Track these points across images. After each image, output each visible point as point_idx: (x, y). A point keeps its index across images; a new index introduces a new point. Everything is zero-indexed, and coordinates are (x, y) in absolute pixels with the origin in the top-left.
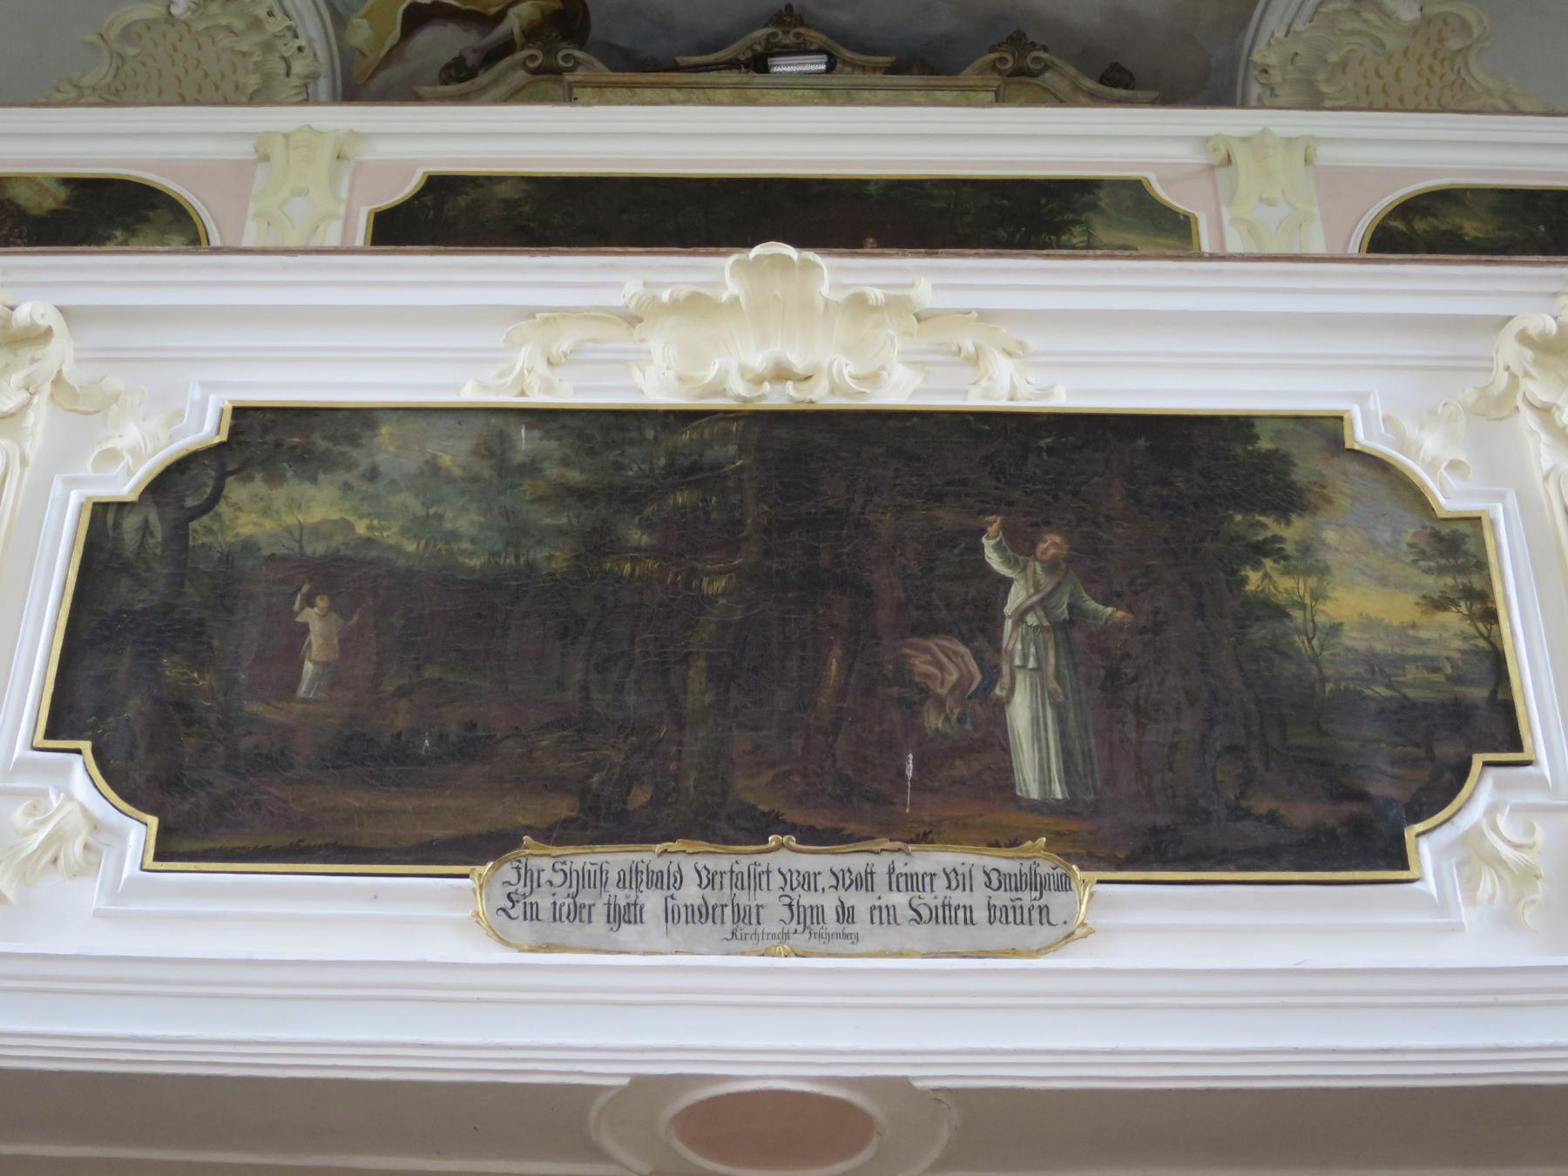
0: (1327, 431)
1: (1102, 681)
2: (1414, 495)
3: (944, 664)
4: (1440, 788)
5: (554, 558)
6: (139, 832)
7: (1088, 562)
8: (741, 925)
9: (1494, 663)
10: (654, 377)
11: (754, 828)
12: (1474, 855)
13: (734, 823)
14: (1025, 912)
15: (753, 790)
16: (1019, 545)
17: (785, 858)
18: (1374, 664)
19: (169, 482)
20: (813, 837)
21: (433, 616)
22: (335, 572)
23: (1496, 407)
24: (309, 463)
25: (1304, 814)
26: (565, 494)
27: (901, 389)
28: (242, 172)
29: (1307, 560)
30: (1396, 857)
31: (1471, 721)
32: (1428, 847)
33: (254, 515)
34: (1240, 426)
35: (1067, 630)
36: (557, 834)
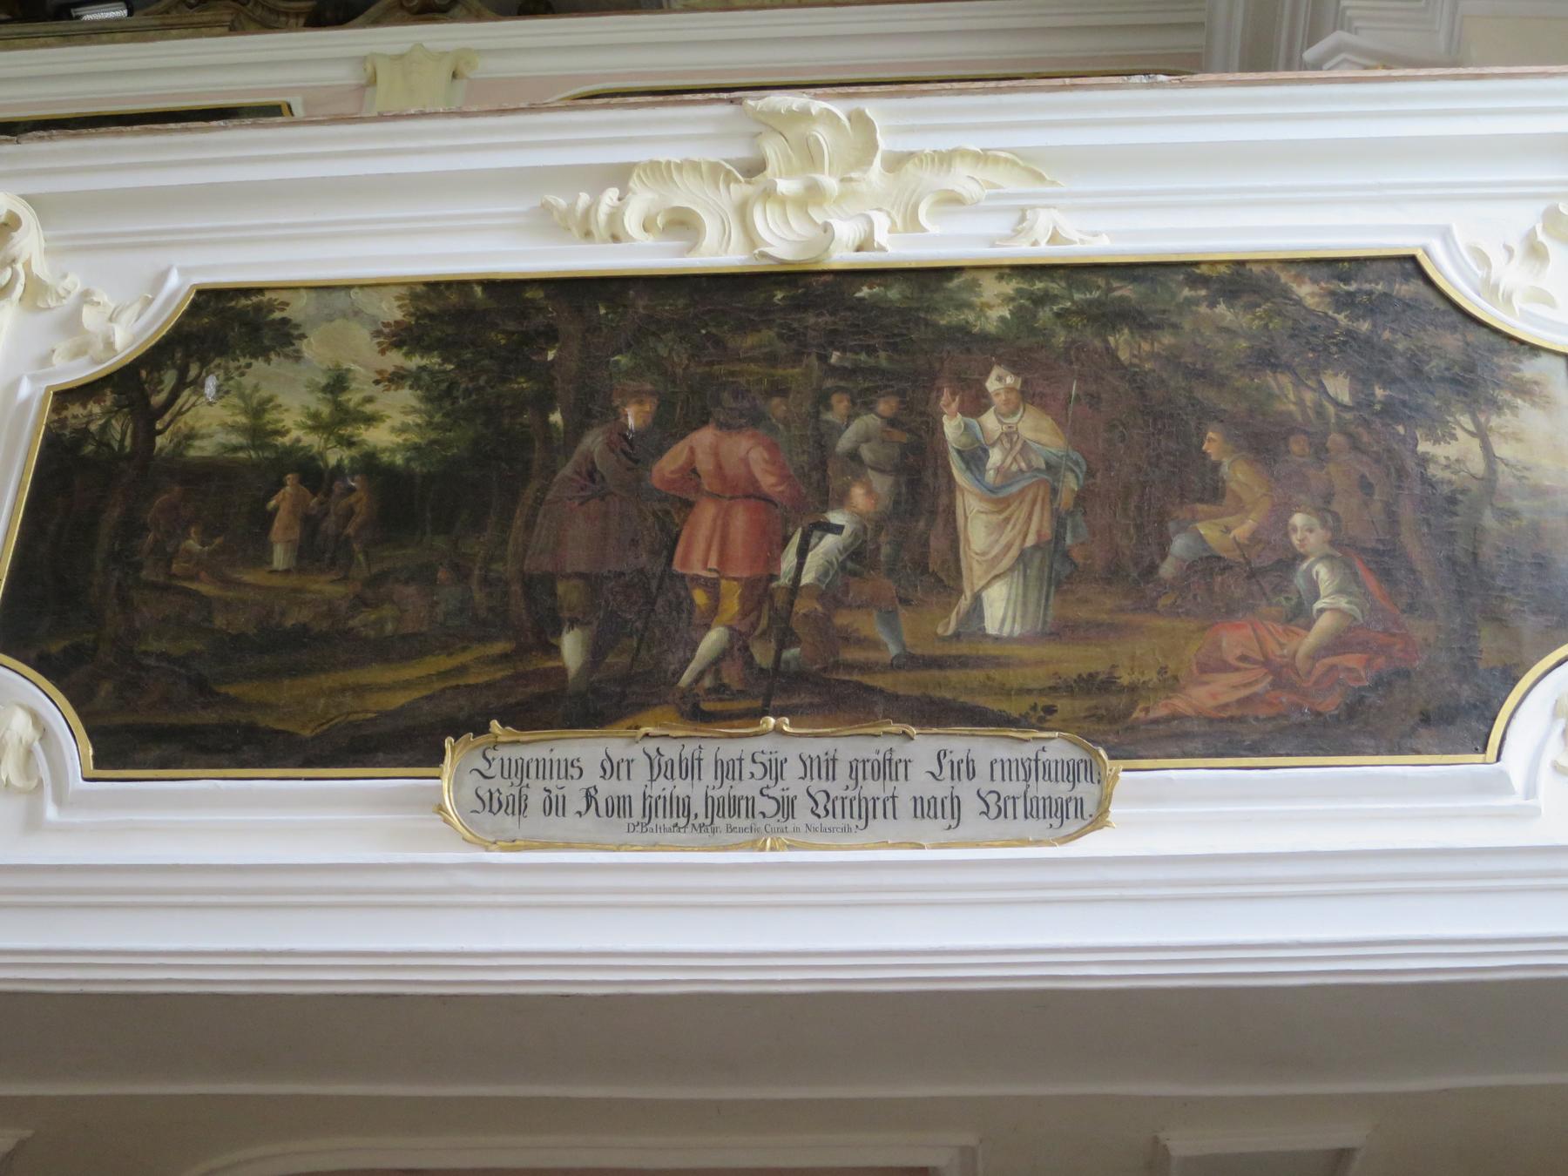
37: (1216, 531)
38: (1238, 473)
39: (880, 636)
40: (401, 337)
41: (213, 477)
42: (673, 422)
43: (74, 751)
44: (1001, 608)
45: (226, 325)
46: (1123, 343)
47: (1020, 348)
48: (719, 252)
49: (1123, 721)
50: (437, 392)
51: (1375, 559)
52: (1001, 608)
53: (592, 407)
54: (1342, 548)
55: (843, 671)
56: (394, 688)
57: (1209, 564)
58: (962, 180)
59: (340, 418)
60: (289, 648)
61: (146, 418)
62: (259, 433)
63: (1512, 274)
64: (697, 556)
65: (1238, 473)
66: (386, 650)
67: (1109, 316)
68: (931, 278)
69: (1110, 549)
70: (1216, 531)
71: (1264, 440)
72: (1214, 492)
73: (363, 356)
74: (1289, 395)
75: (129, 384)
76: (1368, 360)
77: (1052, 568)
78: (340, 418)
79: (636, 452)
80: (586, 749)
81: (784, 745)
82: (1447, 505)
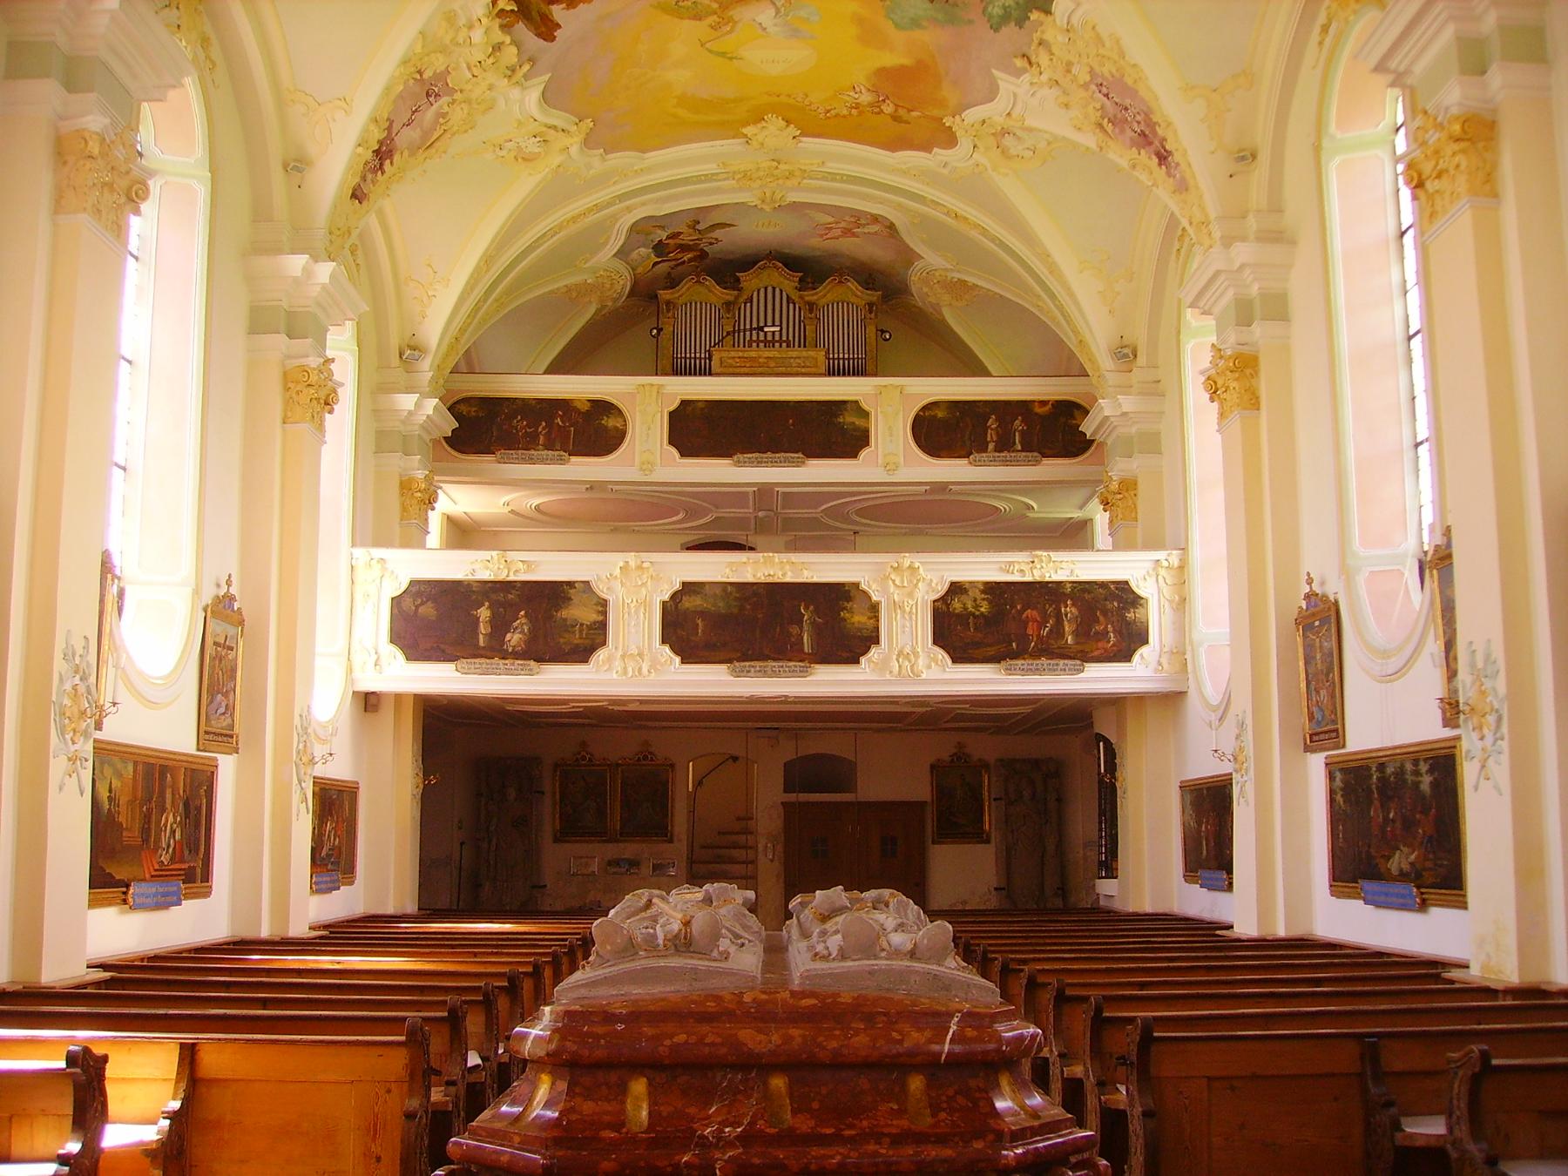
0: (856, 585)
1: (818, 631)
3: (794, 630)
4: (866, 650)
5: (735, 611)
6: (678, 659)
7: (817, 611)
8: (765, 674)
9: (877, 629)
10: (748, 577)
12: (870, 661)
13: (765, 658)
14: (804, 673)
15: (767, 652)
16: (806, 608)
18: (860, 630)
19: (674, 596)
20: (775, 660)
21: (718, 621)
22: (703, 614)
23: (888, 577)
24: (696, 593)
25: (845, 655)
26: (736, 599)
27: (788, 579)
28: (632, 395)
29: (851, 611)
31: (871, 639)
32: (863, 660)
33: (689, 603)
35: (813, 623)
36: (739, 660)
37: (1099, 628)
39: (1054, 644)
40: (983, 592)
41: (959, 616)
42: (1024, 609)
43: (949, 661)
44: (1070, 640)
45: (956, 589)
47: (1071, 596)
49: (1086, 657)
50: (990, 602)
51: (1118, 632)
52: (1070, 640)
53: (1013, 607)
55: (1050, 650)
56: (991, 651)
57: (1097, 633)
59: (977, 607)
60: (977, 645)
62: (966, 609)
63: (1141, 583)
64: (1030, 632)
66: (990, 645)
67: (1084, 591)
68: (1059, 583)
69: (1085, 630)
70: (1099, 628)
71: (1105, 613)
72: (1098, 621)
73: (980, 596)
75: (943, 598)
76: (1120, 599)
77: (1076, 633)
78: (977, 607)
79: (1021, 613)
80: (1020, 662)
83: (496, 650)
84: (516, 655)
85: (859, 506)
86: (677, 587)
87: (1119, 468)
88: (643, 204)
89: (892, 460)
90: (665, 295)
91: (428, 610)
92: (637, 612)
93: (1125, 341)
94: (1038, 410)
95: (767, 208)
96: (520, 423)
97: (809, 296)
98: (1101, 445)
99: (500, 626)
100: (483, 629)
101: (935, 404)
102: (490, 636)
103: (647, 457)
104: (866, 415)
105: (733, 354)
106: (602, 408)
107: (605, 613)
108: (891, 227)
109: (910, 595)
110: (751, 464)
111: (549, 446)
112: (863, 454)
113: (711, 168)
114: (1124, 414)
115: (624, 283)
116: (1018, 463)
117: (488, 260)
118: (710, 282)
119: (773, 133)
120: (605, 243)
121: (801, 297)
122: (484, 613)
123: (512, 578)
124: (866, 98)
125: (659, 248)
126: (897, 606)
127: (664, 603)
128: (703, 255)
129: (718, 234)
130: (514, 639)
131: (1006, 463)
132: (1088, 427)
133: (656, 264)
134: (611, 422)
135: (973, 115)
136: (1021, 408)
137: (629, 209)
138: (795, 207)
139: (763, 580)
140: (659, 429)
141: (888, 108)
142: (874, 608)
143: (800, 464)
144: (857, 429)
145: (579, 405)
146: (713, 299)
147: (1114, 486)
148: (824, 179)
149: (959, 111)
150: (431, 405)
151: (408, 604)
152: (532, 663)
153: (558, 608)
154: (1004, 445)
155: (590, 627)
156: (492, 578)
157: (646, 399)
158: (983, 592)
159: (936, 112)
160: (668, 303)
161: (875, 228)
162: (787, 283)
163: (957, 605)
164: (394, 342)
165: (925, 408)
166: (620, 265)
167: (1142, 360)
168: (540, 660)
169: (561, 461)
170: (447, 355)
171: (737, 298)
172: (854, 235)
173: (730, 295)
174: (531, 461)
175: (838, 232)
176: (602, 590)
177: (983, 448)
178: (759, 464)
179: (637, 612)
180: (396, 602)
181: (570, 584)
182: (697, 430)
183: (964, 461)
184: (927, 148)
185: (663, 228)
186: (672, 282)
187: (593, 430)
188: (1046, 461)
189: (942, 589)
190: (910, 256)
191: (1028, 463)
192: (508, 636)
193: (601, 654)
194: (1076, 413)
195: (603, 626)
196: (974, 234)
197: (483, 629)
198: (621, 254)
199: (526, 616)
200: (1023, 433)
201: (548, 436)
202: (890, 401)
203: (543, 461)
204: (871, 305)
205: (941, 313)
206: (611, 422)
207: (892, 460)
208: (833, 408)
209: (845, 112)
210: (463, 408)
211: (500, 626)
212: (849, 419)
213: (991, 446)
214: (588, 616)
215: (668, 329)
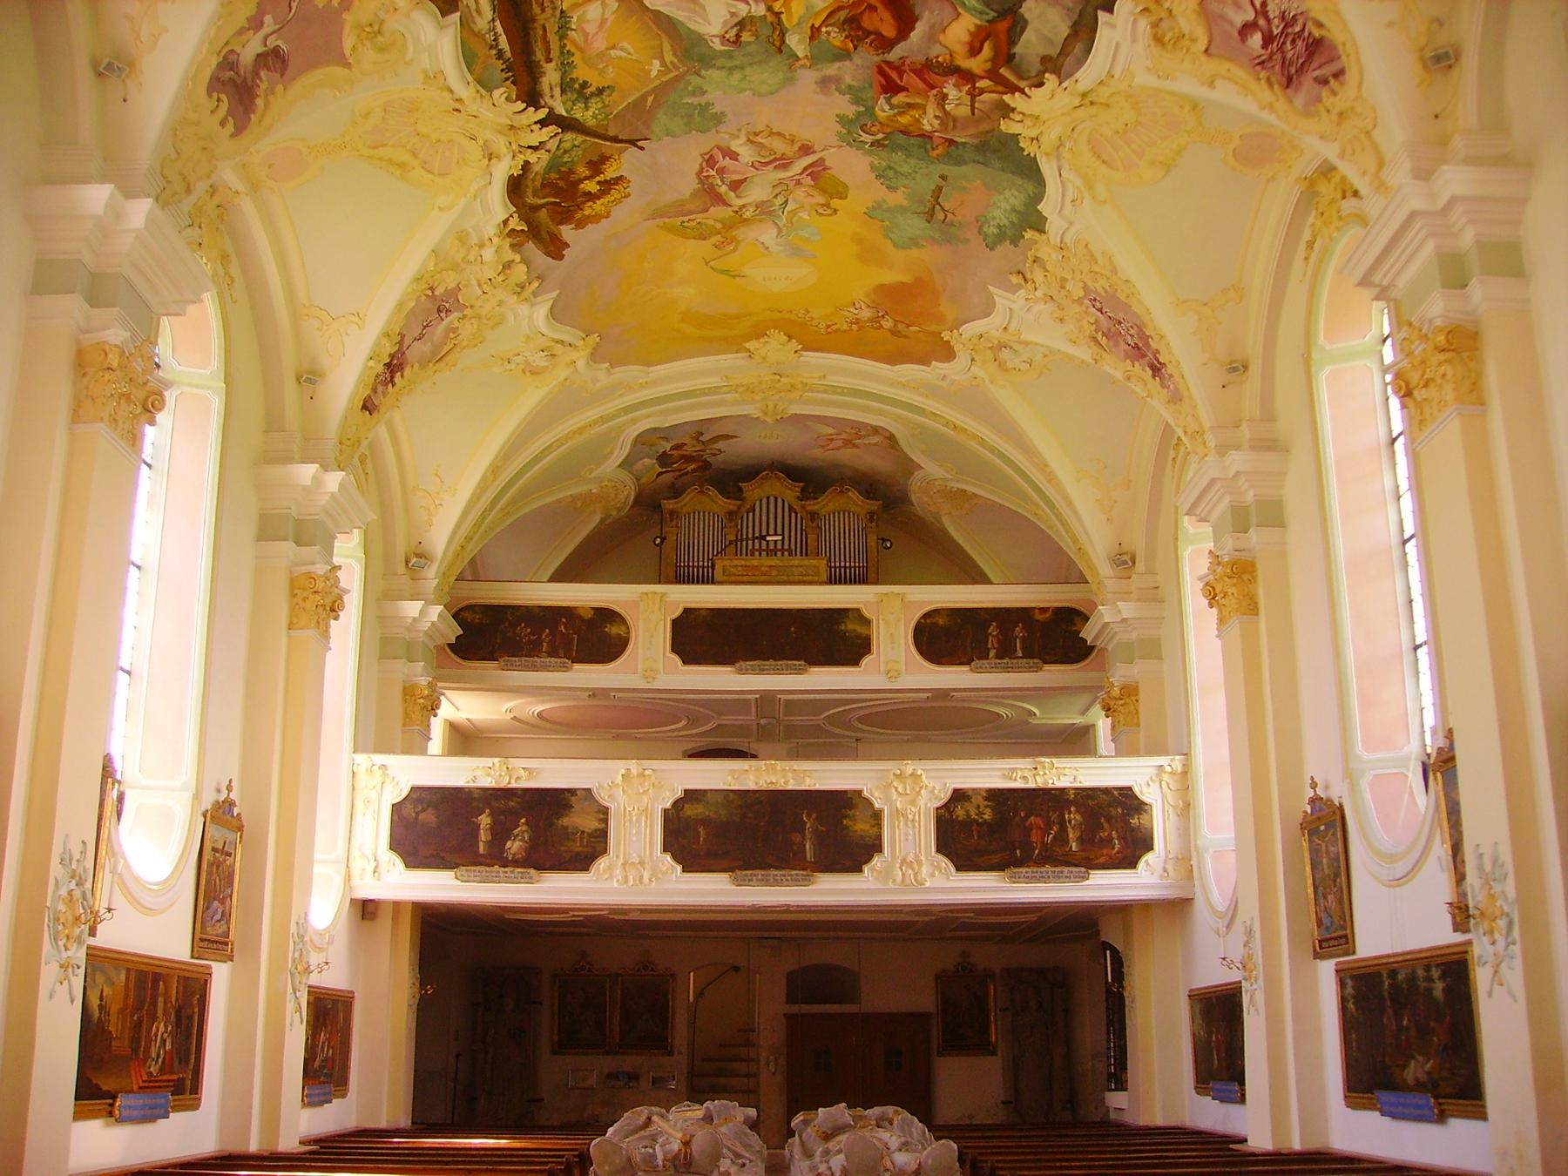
0: (859, 792)
2: (872, 805)
3: (797, 838)
4: (868, 860)
5: (737, 819)
6: (679, 868)
8: (766, 882)
9: (880, 837)
10: (750, 784)
11: (769, 867)
12: (873, 869)
14: (807, 881)
16: (809, 816)
17: (773, 872)
19: (675, 804)
20: (776, 868)
21: (719, 829)
22: (704, 822)
29: (853, 819)
30: (861, 871)
31: (875, 847)
32: (866, 868)
33: (690, 811)
34: (845, 792)
35: (816, 832)
38: (1106, 825)
40: (986, 799)
42: (1028, 816)
43: (953, 869)
44: (1074, 846)
45: (959, 796)
46: (1090, 803)
47: (1075, 802)
48: (1031, 785)
49: (1090, 864)
52: (1074, 846)
53: (1016, 813)
54: (1119, 837)
55: (1055, 858)
56: (995, 859)
57: (1101, 840)
58: (1067, 771)
59: (980, 814)
61: (951, 813)
62: (968, 816)
63: (1145, 790)
65: (1106, 825)
67: (1089, 797)
68: (1063, 790)
74: (1113, 812)
75: (945, 806)
77: (1080, 840)
78: (980, 814)
79: (1024, 820)
80: (1024, 870)
81: (1048, 868)
82: (1133, 830)
83: (496, 858)
84: (516, 863)
85: (862, 713)
86: (680, 794)
87: (1120, 674)
88: (648, 416)
89: (894, 667)
90: (669, 505)
91: (429, 817)
92: (638, 820)
93: (1125, 548)
94: (1039, 617)
95: (769, 420)
96: (524, 630)
97: (811, 506)
98: (1103, 650)
99: (501, 833)
100: (484, 836)
101: (936, 611)
102: (490, 844)
103: (650, 665)
104: (867, 622)
105: (736, 563)
106: (606, 615)
107: (606, 821)
108: (891, 438)
109: (913, 802)
110: (753, 671)
111: (553, 653)
112: (865, 661)
113: (713, 381)
114: (1124, 620)
115: (629, 493)
116: (1018, 669)
117: (494, 470)
118: (713, 492)
119: (775, 347)
120: (611, 453)
121: (803, 507)
122: (485, 820)
123: (513, 785)
124: (866, 314)
125: (663, 459)
126: (898, 813)
127: (665, 811)
128: (706, 466)
129: (721, 445)
130: (514, 846)
131: (1007, 669)
132: (1088, 633)
133: (659, 474)
134: (614, 630)
135: (970, 329)
136: (1022, 615)
137: (634, 421)
138: (797, 419)
139: (765, 787)
140: (664, 636)
141: (887, 324)
142: (877, 816)
143: (800, 672)
144: (859, 636)
145: (582, 613)
146: (716, 509)
147: (1116, 692)
148: (825, 392)
149: (957, 325)
150: (436, 611)
151: (409, 811)
152: (532, 871)
153: (559, 816)
154: (1005, 652)
155: (591, 835)
156: (493, 785)
157: (649, 607)
158: (986, 799)
159: (934, 327)
160: (672, 512)
161: (875, 439)
162: (789, 492)
163: (960, 812)
164: (401, 550)
165: (926, 616)
166: (626, 477)
167: (1140, 566)
168: (541, 868)
169: (565, 668)
170: (452, 564)
171: (739, 507)
172: (854, 446)
173: (732, 505)
174: (535, 668)
175: (840, 443)
176: (603, 798)
177: (984, 656)
178: (761, 671)
179: (638, 820)
180: (397, 808)
181: (572, 792)
182: (699, 638)
183: (966, 668)
184: (924, 361)
185: (667, 439)
186: (676, 492)
187: (597, 638)
188: (1047, 667)
189: (944, 797)
190: (910, 467)
191: (1030, 669)
192: (509, 844)
193: (602, 863)
194: (1077, 620)
195: (603, 834)
196: (973, 444)
197: (484, 836)
198: (626, 464)
199: (526, 823)
200: (1024, 640)
201: (551, 642)
202: (892, 609)
203: (545, 668)
204: (871, 515)
205: (940, 522)
206: (614, 630)
207: (894, 667)
208: (834, 617)
209: (845, 327)
210: (468, 616)
211: (501, 833)
212: (851, 626)
213: (992, 654)
214: (590, 824)
215: (671, 538)
